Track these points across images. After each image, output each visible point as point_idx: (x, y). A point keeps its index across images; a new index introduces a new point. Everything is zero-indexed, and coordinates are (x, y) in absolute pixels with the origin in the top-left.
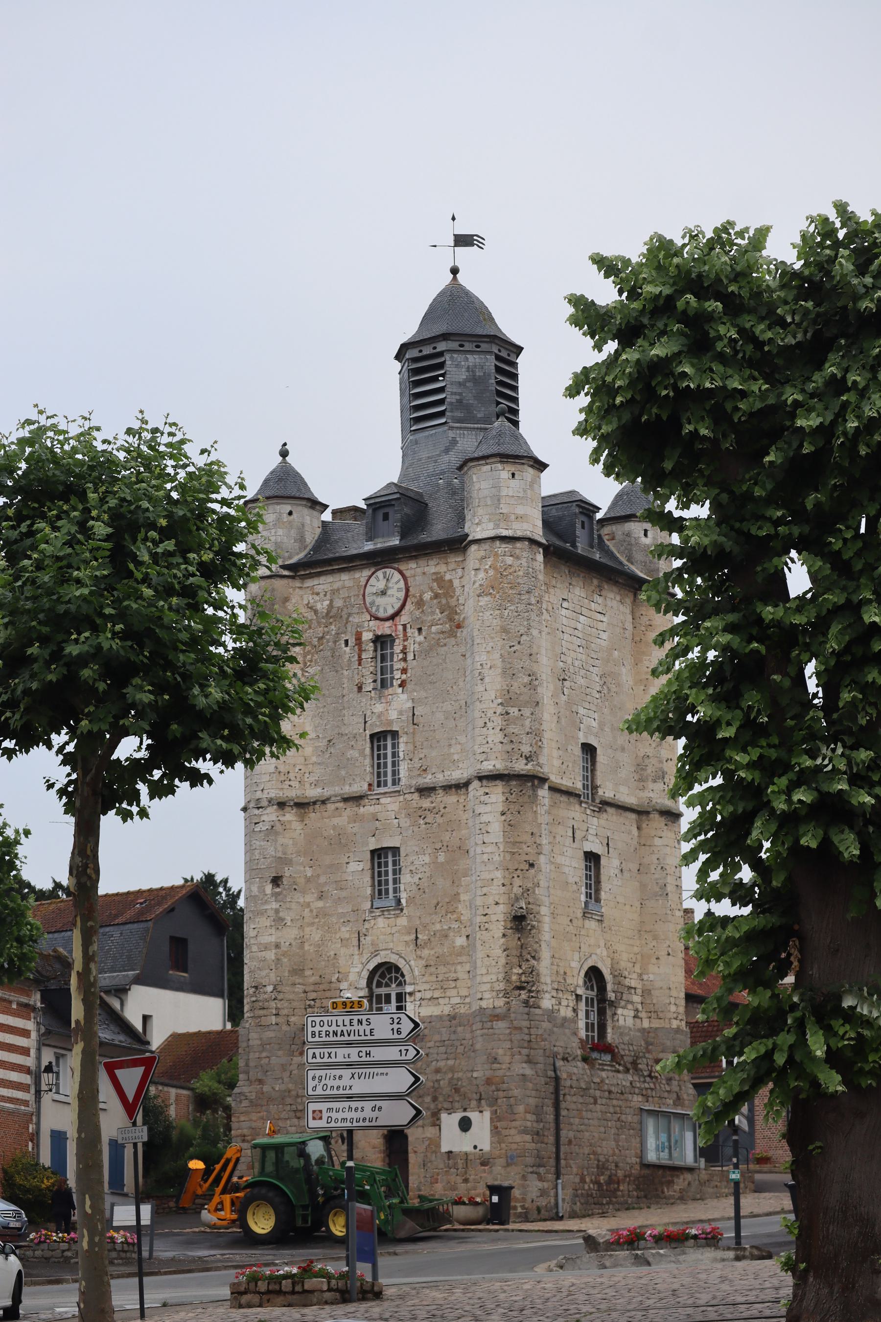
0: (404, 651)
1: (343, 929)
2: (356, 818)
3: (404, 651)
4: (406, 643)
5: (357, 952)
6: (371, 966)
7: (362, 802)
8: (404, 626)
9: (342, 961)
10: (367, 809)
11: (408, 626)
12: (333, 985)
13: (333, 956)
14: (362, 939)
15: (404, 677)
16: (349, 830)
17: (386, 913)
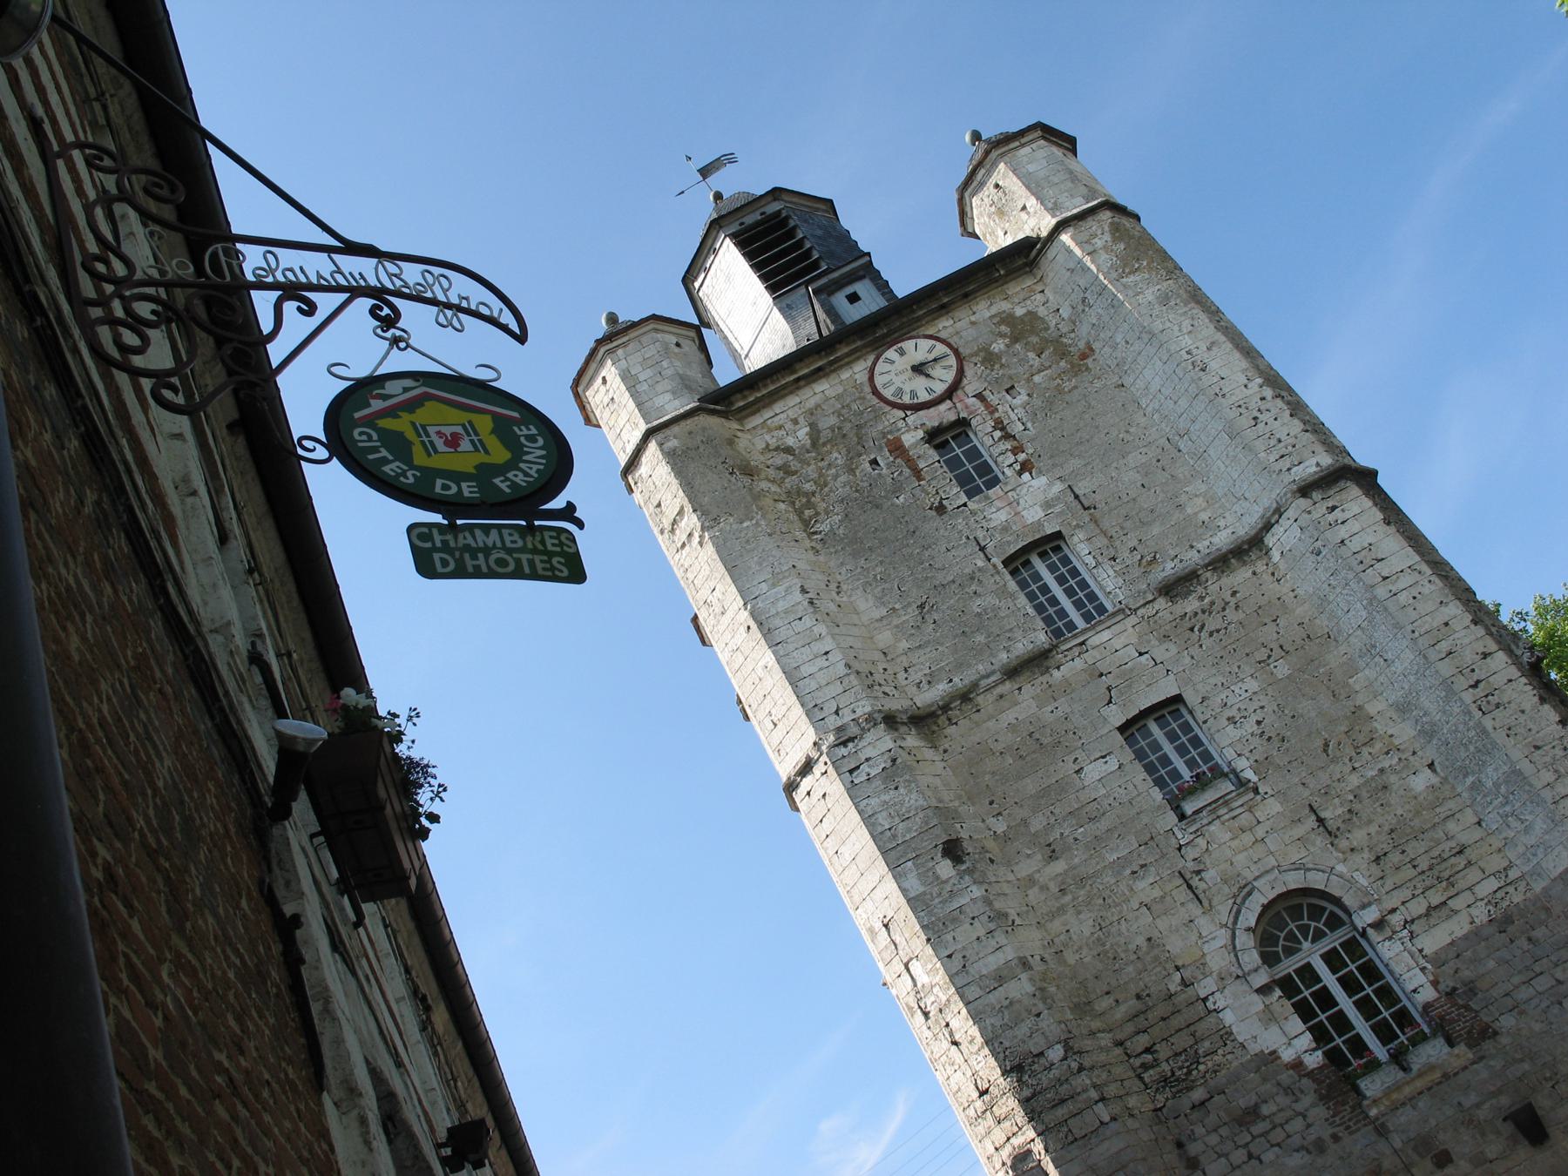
0: (999, 425)
1: (1141, 885)
2: (1052, 693)
3: (999, 425)
4: (997, 415)
5: (1194, 908)
6: (1250, 918)
7: (1051, 662)
8: (980, 396)
9: (1175, 945)
10: (1069, 669)
11: (987, 393)
12: (1177, 1000)
13: (1144, 945)
14: (1195, 882)
15: (1022, 457)
16: (1049, 718)
17: (1222, 811)
